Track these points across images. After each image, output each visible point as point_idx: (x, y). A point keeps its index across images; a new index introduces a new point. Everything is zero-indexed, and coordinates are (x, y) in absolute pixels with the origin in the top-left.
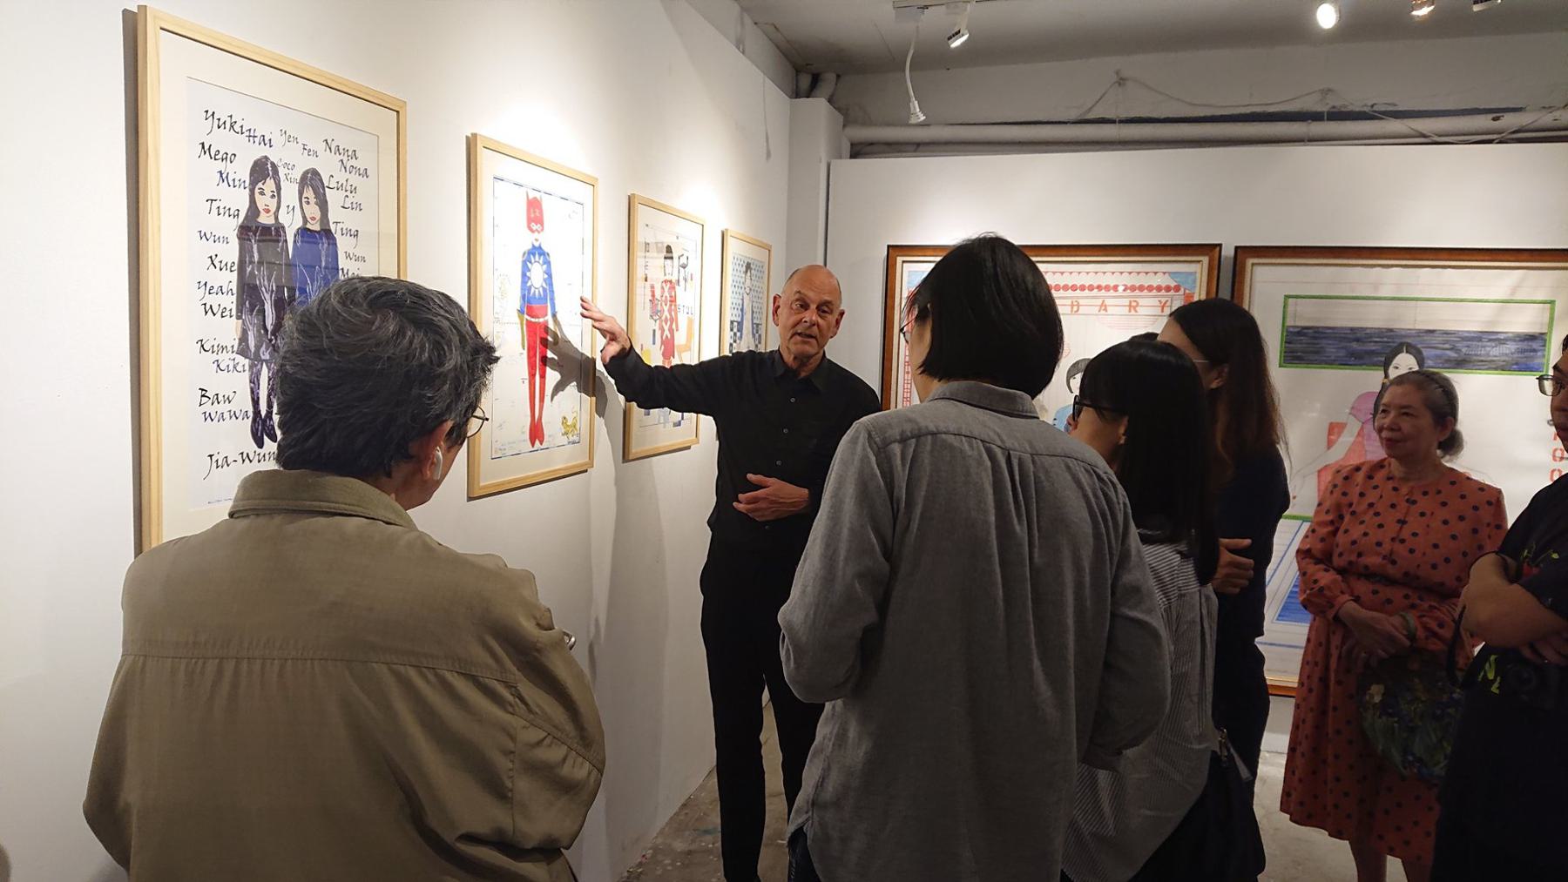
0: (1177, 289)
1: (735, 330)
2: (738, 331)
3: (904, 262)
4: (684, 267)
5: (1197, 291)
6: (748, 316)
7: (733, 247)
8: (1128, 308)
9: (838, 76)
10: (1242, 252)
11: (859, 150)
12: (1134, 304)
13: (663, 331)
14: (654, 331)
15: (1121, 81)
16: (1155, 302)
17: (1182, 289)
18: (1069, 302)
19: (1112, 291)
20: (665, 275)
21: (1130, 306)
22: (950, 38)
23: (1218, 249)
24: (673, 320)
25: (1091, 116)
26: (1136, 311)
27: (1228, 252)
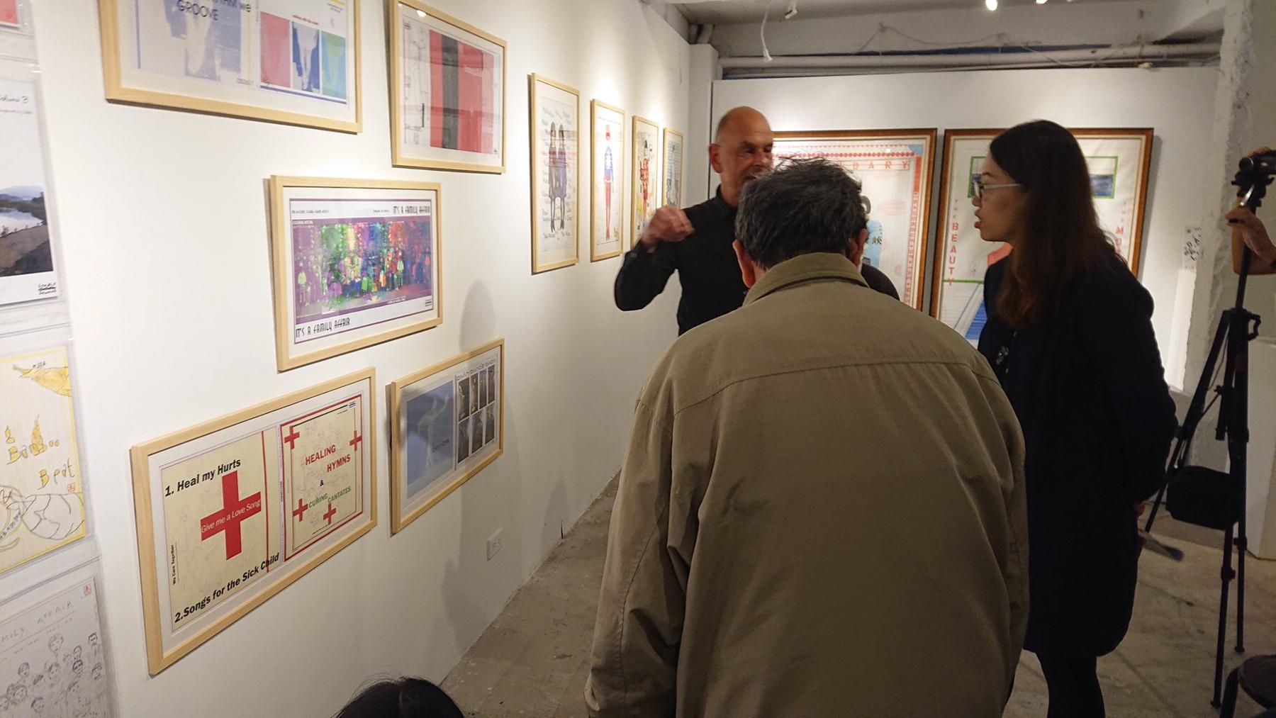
0: (912, 154)
4: (651, 150)
5: (923, 155)
6: (673, 177)
7: (667, 134)
9: (714, 26)
10: (949, 133)
11: (728, 74)
15: (883, 29)
16: (900, 162)
18: (852, 163)
20: (645, 155)
22: (786, 14)
24: (647, 179)
25: (865, 50)
27: (941, 133)
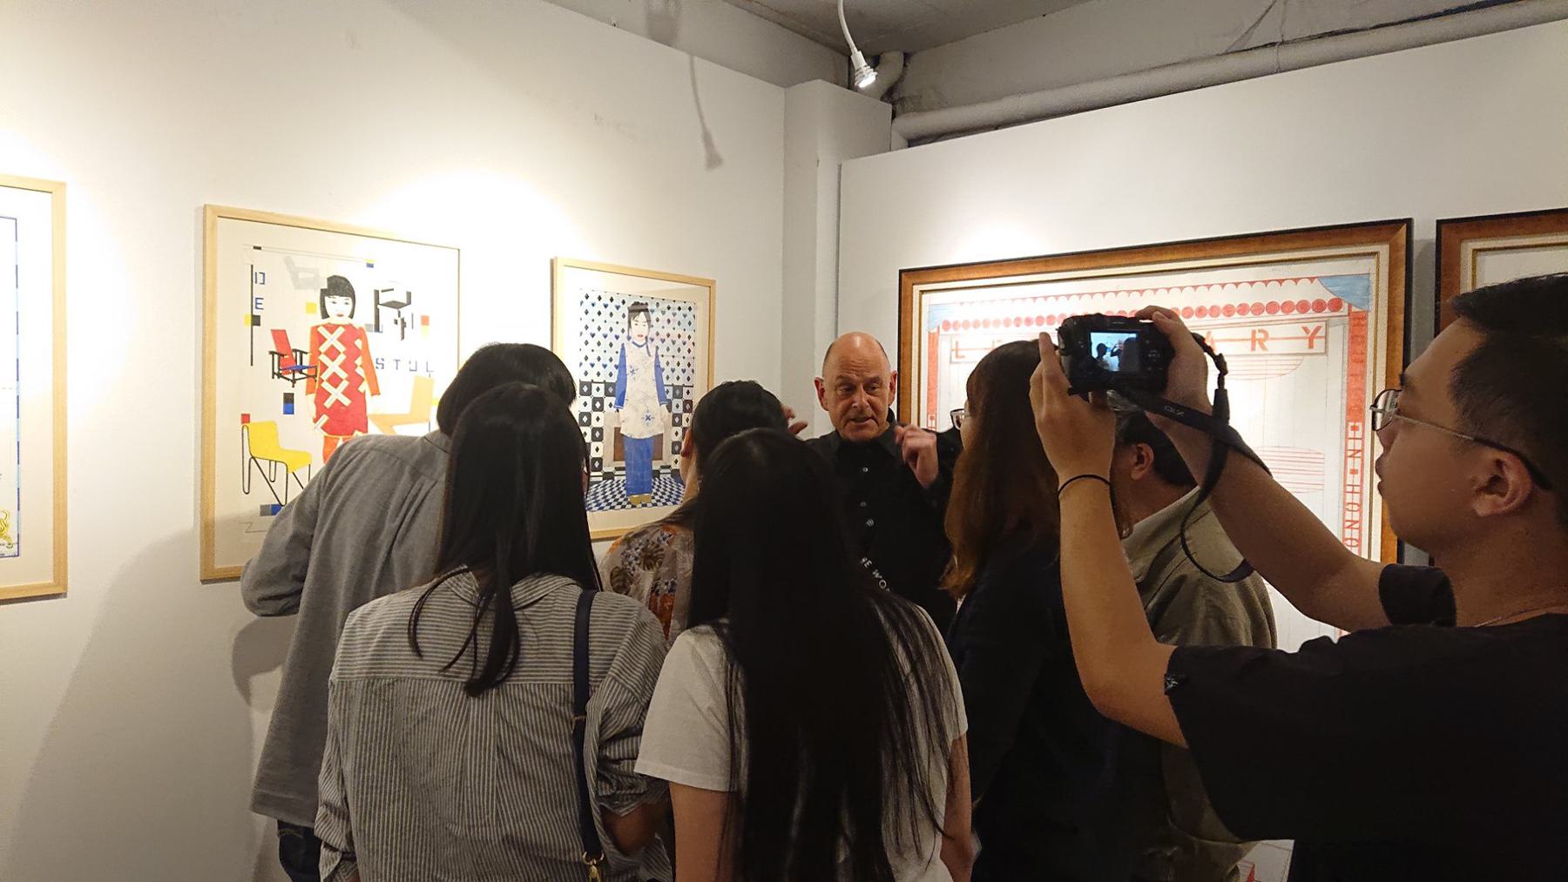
0: (1336, 305)
1: (601, 394)
2: (607, 394)
3: (922, 292)
5: (1372, 308)
8: (1249, 343)
9: (907, 56)
10: (1452, 230)
12: (1259, 336)
13: (323, 395)
14: (289, 399)
16: (1297, 330)
17: (1345, 305)
19: (1222, 316)
20: (325, 315)
21: (1253, 340)
23: (1404, 227)
26: (1264, 348)
27: (1424, 233)
